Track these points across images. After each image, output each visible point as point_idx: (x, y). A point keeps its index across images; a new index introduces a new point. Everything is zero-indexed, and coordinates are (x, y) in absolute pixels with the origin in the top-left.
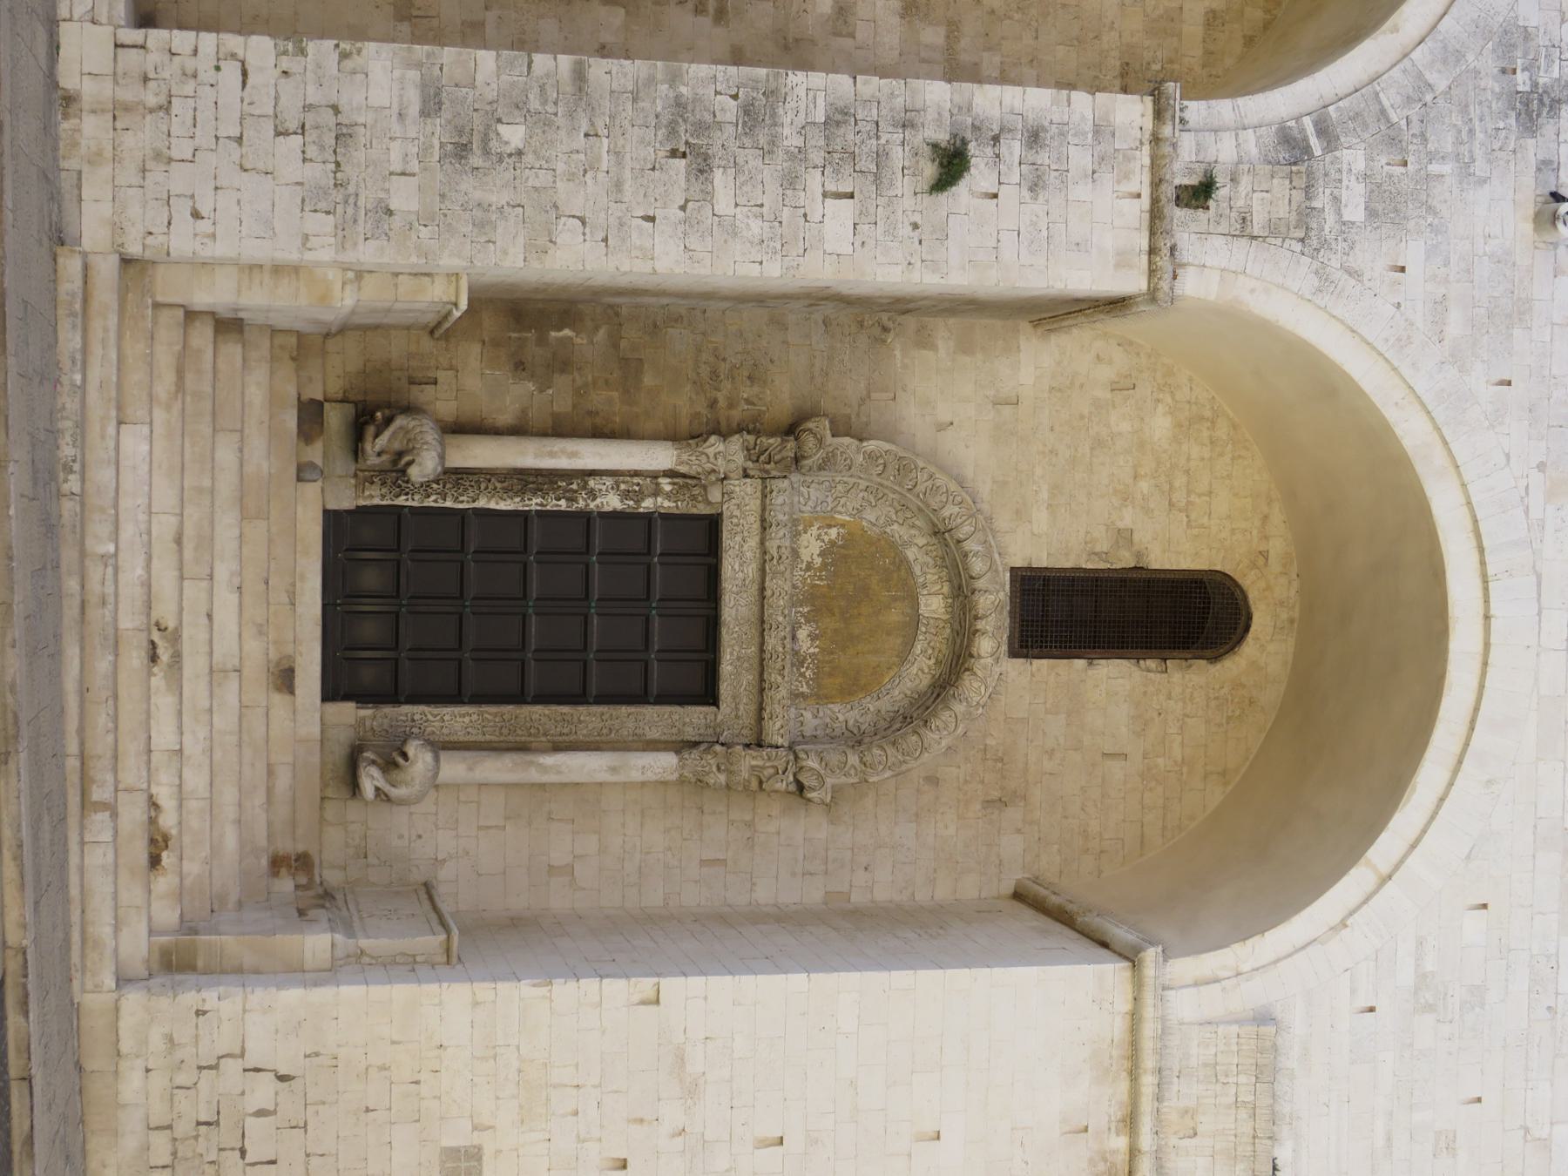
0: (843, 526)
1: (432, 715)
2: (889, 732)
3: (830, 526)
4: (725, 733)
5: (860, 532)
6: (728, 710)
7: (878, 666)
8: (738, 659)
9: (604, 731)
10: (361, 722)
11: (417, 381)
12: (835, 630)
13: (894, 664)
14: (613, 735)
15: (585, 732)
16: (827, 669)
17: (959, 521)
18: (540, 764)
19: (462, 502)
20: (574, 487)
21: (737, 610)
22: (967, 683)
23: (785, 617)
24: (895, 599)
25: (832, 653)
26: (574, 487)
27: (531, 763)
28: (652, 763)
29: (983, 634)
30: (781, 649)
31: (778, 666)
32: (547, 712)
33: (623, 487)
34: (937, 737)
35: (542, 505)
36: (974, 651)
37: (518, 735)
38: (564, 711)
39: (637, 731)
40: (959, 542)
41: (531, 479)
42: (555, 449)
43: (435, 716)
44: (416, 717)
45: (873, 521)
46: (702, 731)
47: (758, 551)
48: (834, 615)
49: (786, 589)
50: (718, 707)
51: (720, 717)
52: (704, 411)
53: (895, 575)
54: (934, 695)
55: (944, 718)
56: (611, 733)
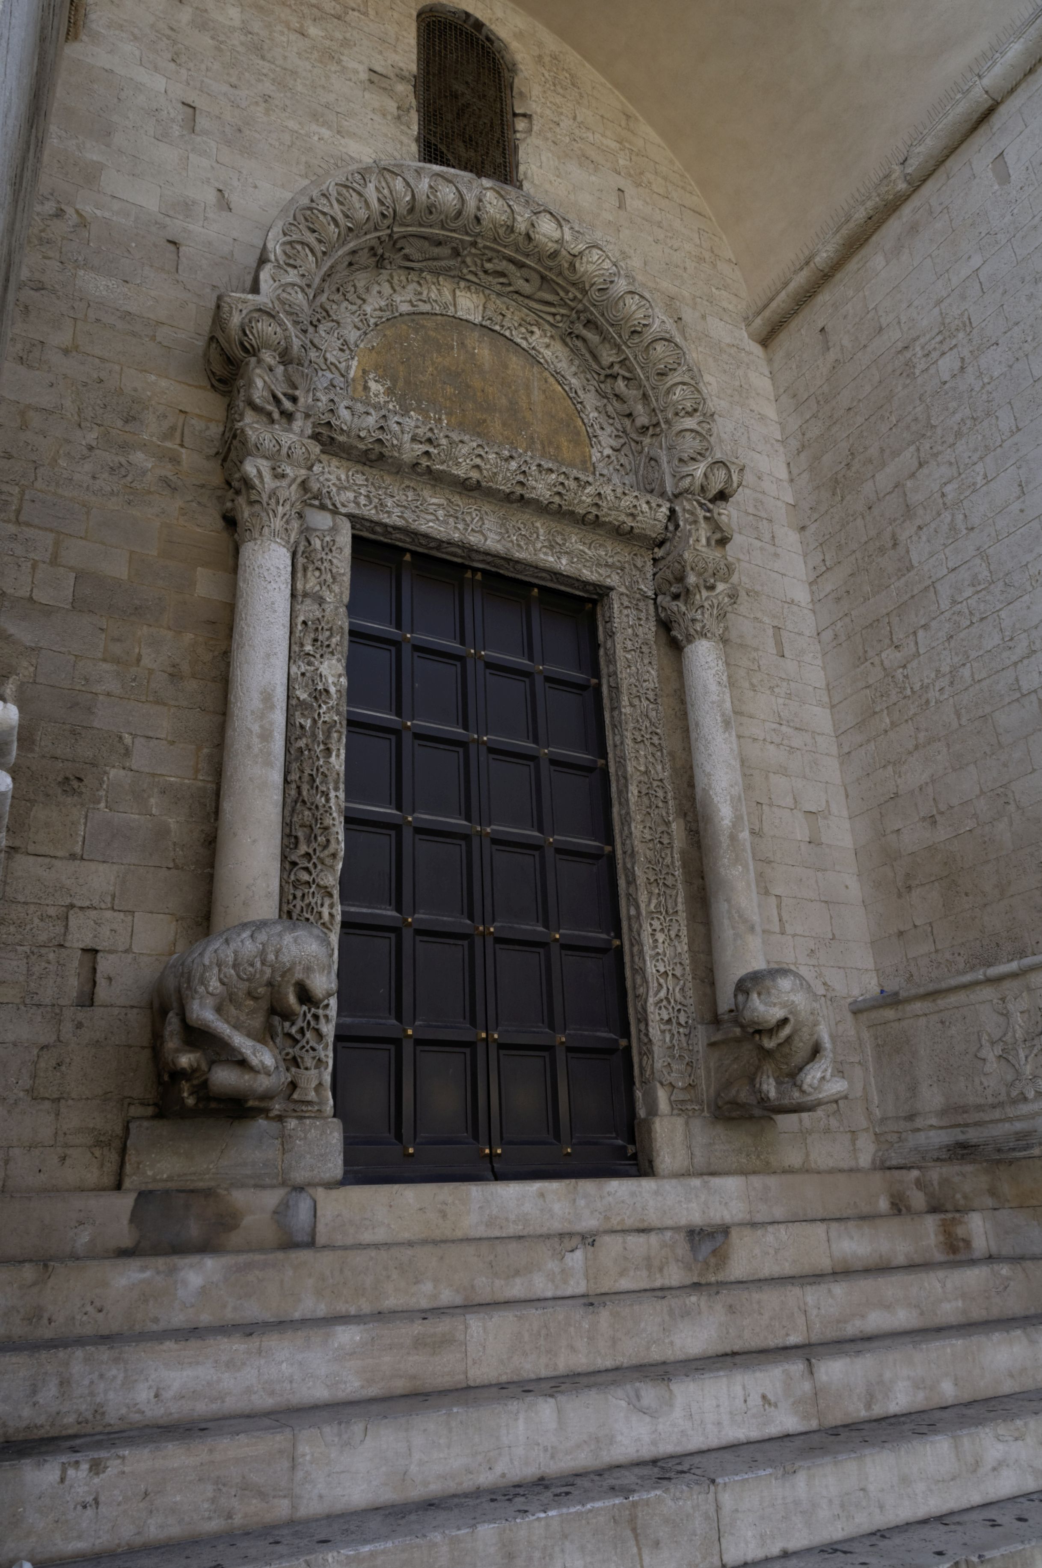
0: (364, 372)
1: (656, 994)
2: (632, 393)
3: (366, 388)
4: (643, 587)
5: (374, 354)
6: (616, 577)
7: (544, 391)
8: (551, 547)
9: (656, 740)
10: (678, 1107)
11: (87, 988)
12: (504, 424)
13: (541, 373)
14: (658, 731)
15: (659, 767)
16: (552, 451)
17: (386, 192)
18: (734, 826)
19: (331, 915)
20: (308, 723)
21: (490, 530)
22: (591, 268)
23: (512, 457)
24: (462, 344)
25: (532, 438)
26: (308, 723)
27: (733, 838)
28: (713, 672)
29: (533, 225)
30: (554, 476)
31: (573, 484)
32: (639, 817)
33: (308, 648)
34: (657, 322)
35: (337, 782)
36: (552, 246)
37: (673, 862)
38: (636, 792)
39: (651, 695)
40: (411, 210)
41: (293, 792)
42: (256, 728)
43: (660, 985)
44: (666, 1017)
45: (358, 333)
46: (643, 615)
47: (407, 483)
48: (485, 421)
49: (475, 444)
50: (611, 589)
51: (623, 589)
52: (179, 503)
53: (432, 333)
54: (585, 333)
55: (634, 308)
56: (657, 734)
